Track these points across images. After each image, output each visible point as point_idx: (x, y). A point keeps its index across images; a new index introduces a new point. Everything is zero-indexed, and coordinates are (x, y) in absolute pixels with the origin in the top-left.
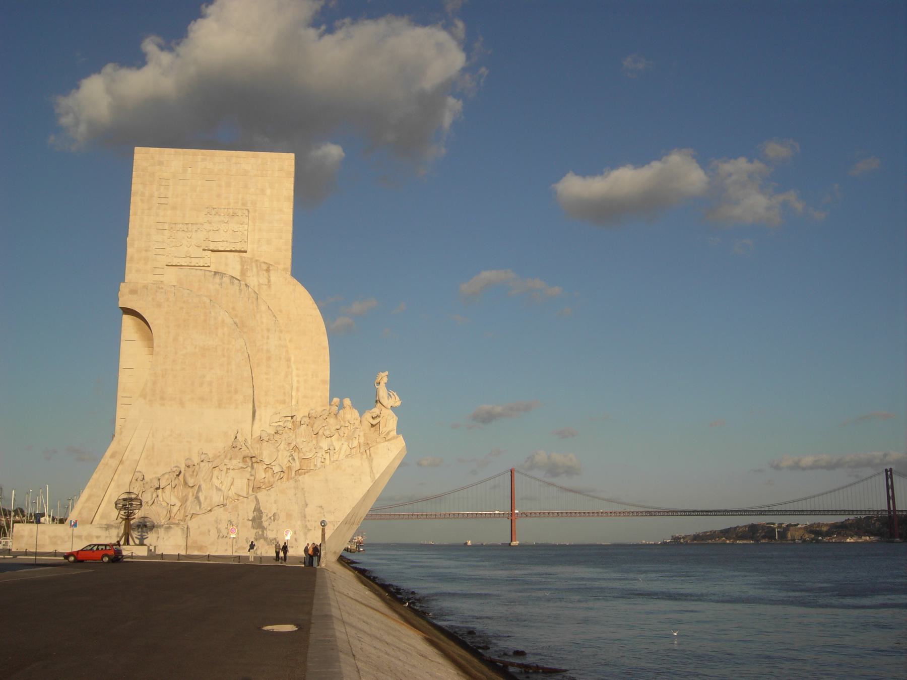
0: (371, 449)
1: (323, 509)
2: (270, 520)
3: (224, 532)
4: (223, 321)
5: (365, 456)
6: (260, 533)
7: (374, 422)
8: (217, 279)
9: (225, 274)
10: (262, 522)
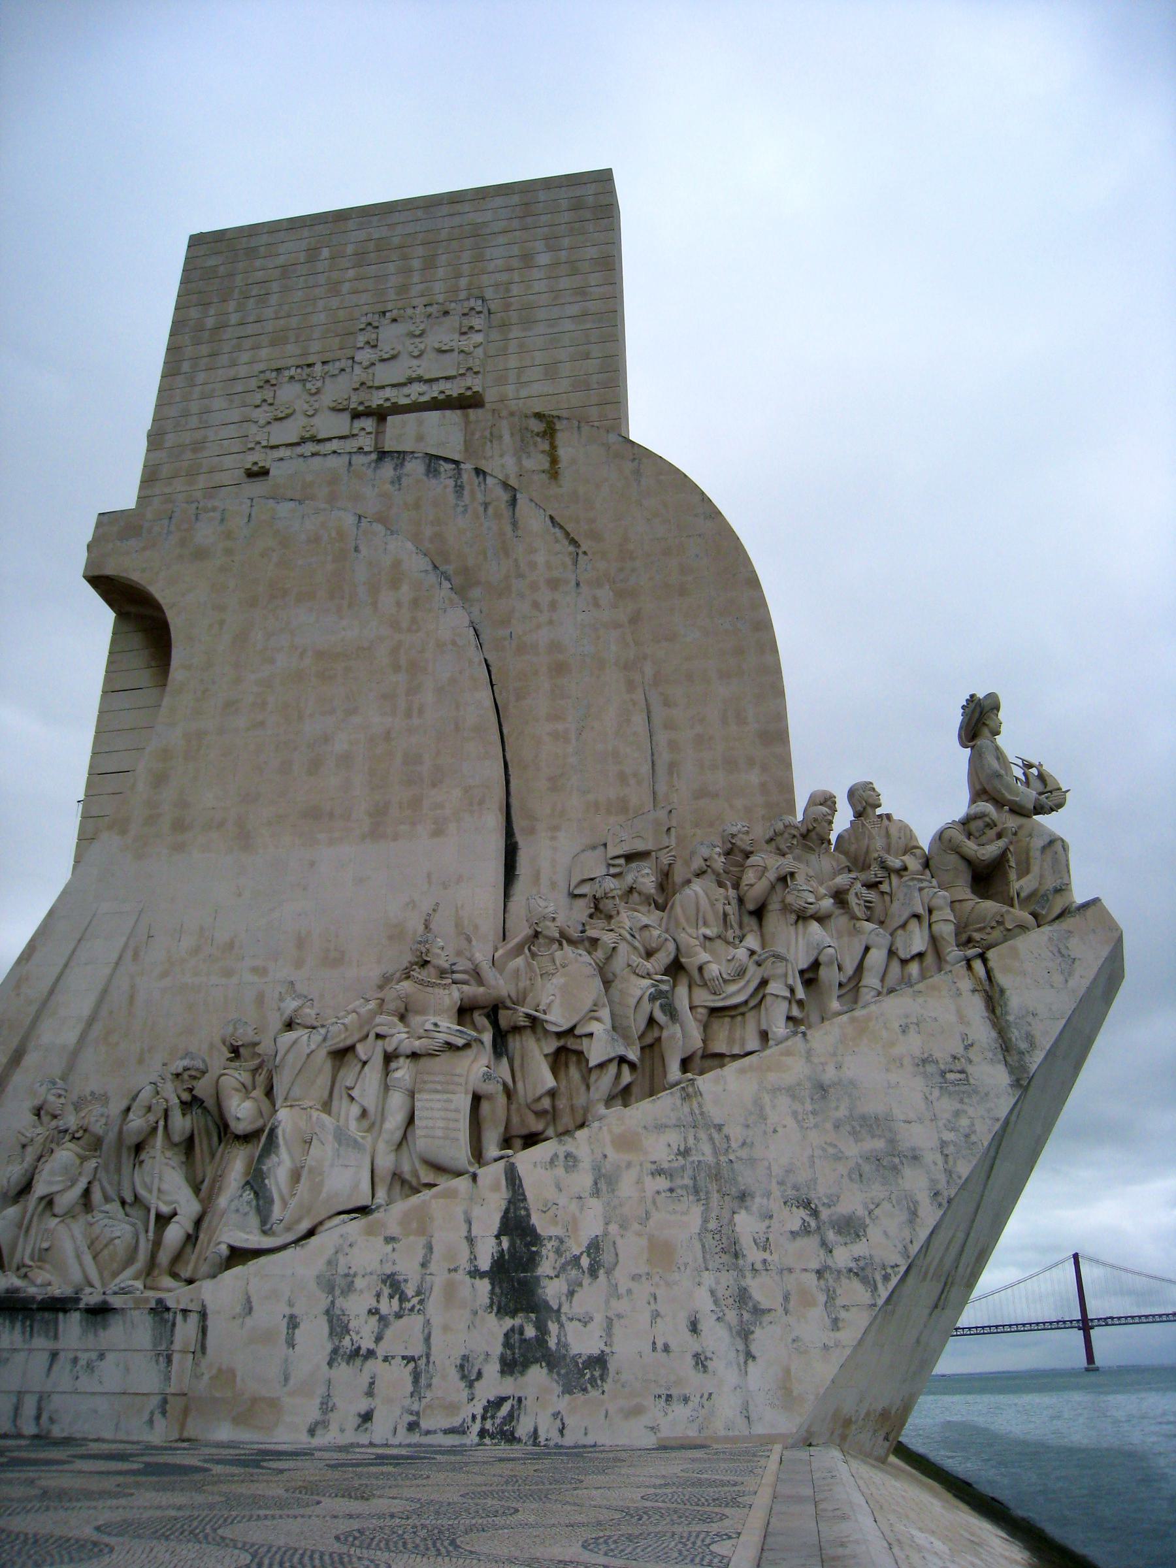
0: (991, 954)
1: (815, 1213)
2: (574, 1273)
3: (364, 1333)
4: (397, 564)
5: (966, 984)
6: (530, 1332)
7: (990, 851)
8: (388, 470)
9: (413, 452)
10: (538, 1278)
